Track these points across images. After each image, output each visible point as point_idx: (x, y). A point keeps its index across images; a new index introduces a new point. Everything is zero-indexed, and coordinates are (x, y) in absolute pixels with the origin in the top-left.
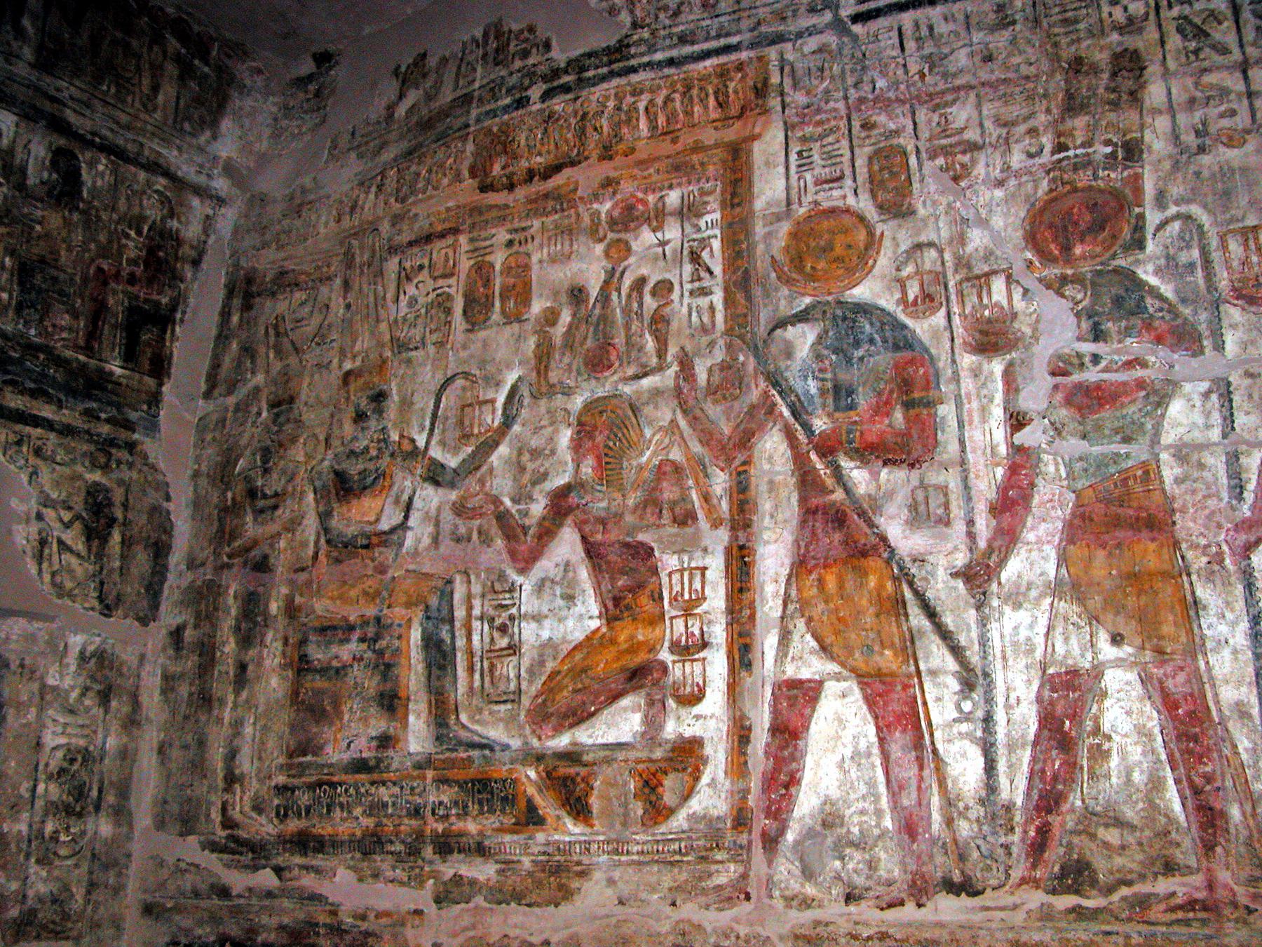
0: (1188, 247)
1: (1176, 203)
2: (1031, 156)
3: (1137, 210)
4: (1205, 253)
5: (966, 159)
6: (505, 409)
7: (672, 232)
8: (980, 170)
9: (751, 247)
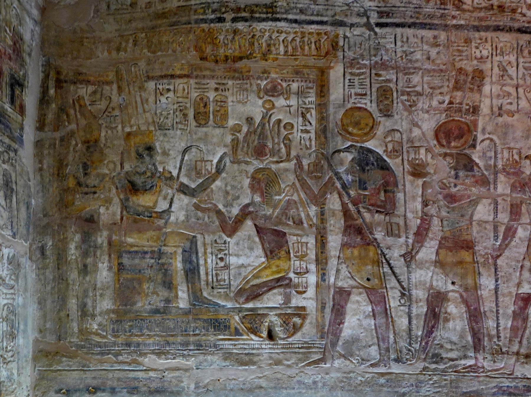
0: (491, 151)
1: (489, 134)
2: (440, 103)
3: (475, 133)
4: (496, 153)
5: (415, 98)
6: (217, 166)
7: (293, 101)
8: (420, 105)
9: (328, 116)
